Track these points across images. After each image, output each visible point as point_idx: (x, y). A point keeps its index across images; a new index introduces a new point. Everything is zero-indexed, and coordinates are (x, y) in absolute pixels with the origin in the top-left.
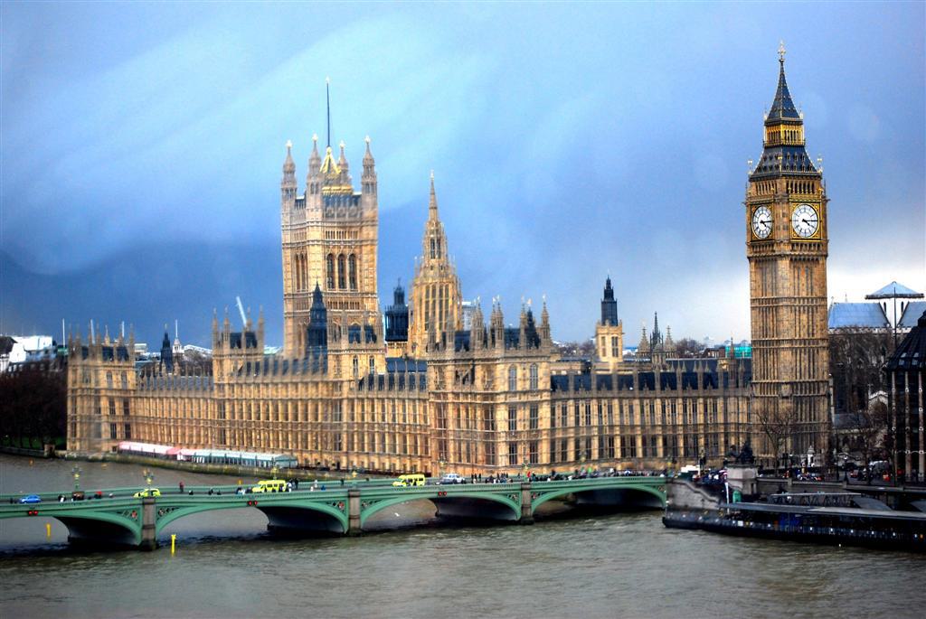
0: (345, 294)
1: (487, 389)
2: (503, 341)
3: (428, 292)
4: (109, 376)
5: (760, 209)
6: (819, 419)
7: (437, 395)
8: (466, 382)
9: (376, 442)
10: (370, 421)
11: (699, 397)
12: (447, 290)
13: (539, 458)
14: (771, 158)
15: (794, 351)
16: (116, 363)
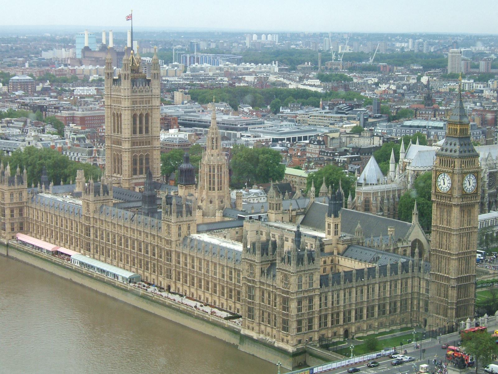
0: (142, 137)
1: (285, 288)
2: (296, 262)
3: (210, 169)
4: (12, 195)
5: (443, 174)
6: (470, 296)
7: (249, 281)
8: (269, 277)
9: (195, 282)
10: (191, 267)
11: (398, 280)
12: (221, 168)
13: (313, 327)
14: (451, 144)
15: (459, 259)
16: (16, 187)
